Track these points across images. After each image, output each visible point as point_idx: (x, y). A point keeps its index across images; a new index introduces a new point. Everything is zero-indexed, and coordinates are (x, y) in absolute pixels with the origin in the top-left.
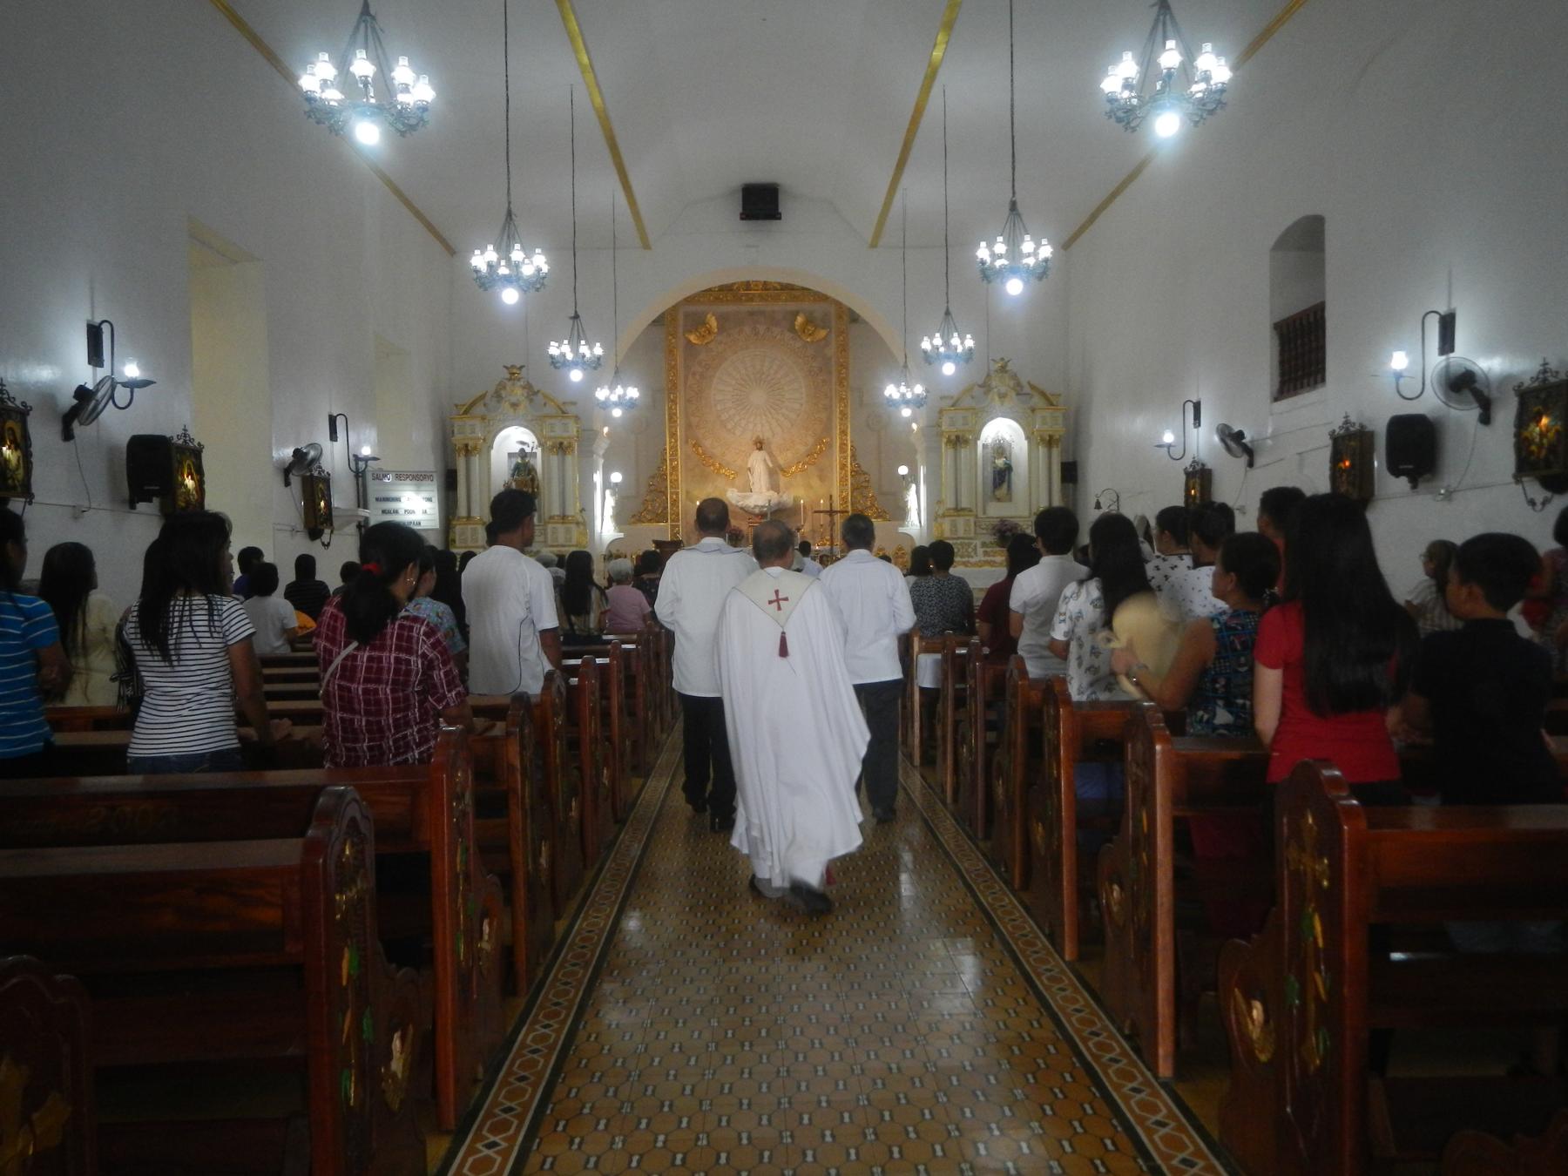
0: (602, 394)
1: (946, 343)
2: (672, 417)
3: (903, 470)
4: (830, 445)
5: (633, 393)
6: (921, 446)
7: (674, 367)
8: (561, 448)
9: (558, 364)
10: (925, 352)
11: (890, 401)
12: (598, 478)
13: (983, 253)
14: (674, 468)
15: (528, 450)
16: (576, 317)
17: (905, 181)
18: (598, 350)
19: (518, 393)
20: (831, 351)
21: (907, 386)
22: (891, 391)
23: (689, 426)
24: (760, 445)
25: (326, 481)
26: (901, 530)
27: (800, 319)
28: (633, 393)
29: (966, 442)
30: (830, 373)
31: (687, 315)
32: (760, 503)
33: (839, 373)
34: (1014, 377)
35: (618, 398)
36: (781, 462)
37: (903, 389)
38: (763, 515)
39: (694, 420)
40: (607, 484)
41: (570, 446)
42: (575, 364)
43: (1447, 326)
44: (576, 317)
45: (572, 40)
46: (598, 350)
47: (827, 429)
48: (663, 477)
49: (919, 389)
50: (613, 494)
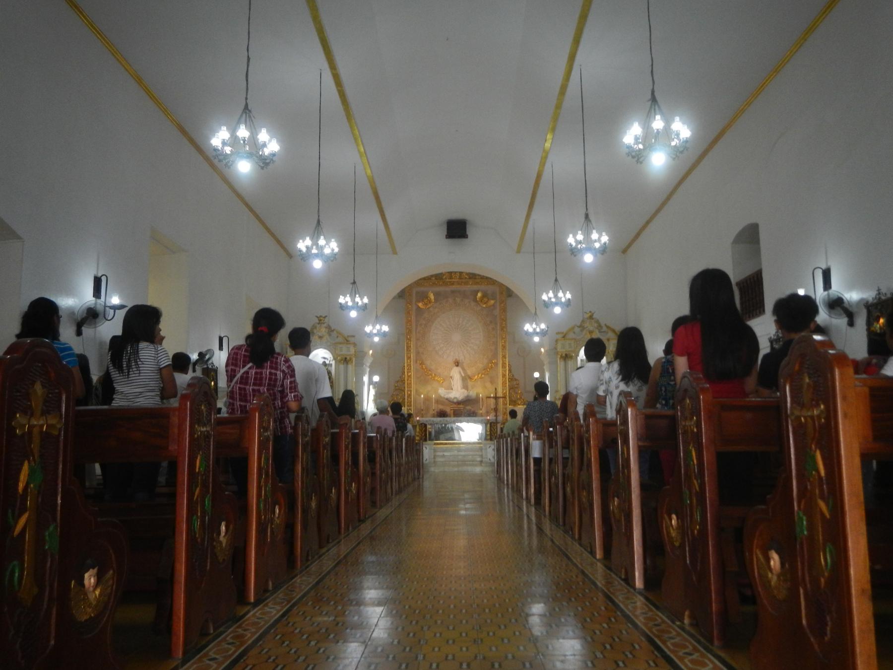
0: (368, 329)
1: (556, 296)
2: (408, 348)
4: (496, 364)
5: (386, 328)
6: (546, 362)
7: (410, 321)
8: (346, 361)
9: (343, 307)
10: (544, 301)
11: (527, 333)
12: (366, 379)
13: (571, 240)
14: (409, 377)
15: (327, 362)
16: (354, 283)
17: (534, 216)
18: (366, 300)
19: (323, 331)
20: (497, 312)
21: (537, 324)
22: (528, 327)
23: (418, 353)
24: (457, 364)
25: (215, 371)
27: (479, 295)
28: (386, 328)
29: (571, 357)
31: (417, 293)
34: (597, 321)
35: (377, 331)
36: (469, 373)
37: (534, 326)
38: (459, 403)
40: (371, 382)
41: (351, 359)
42: (352, 308)
43: (827, 275)
44: (354, 283)
45: (355, 139)
46: (366, 300)
47: (495, 355)
48: (403, 381)
49: (543, 326)
50: (374, 388)
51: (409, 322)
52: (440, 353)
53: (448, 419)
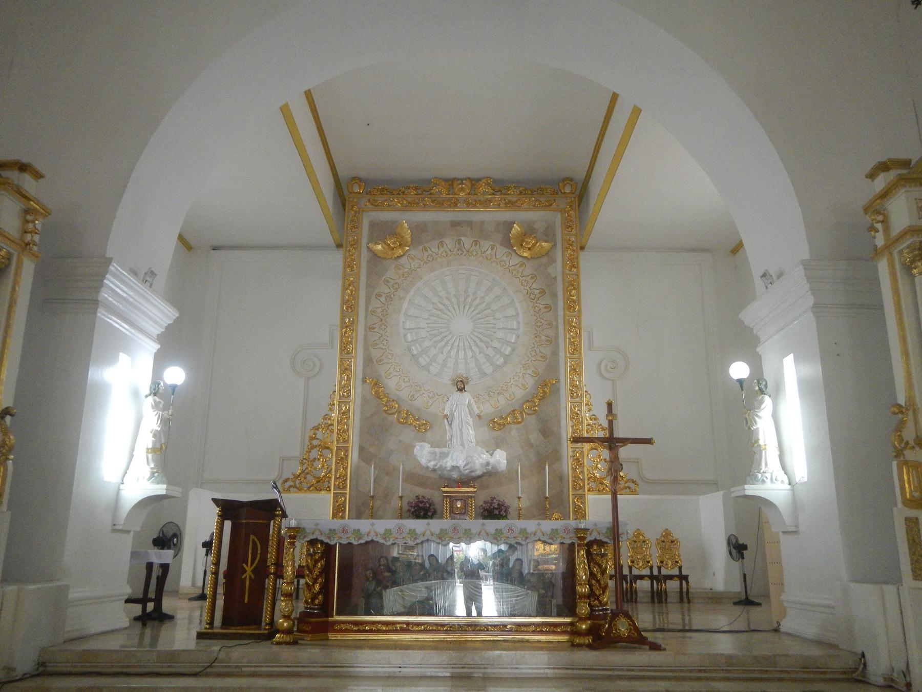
3: (739, 370)
14: (345, 414)
20: (557, 270)
23: (368, 360)
24: (461, 386)
26: (751, 490)
30: (554, 295)
31: (373, 225)
32: (461, 463)
33: (567, 298)
39: (375, 353)
50: (156, 406)
51: (350, 285)
52: (423, 361)
53: (435, 525)
